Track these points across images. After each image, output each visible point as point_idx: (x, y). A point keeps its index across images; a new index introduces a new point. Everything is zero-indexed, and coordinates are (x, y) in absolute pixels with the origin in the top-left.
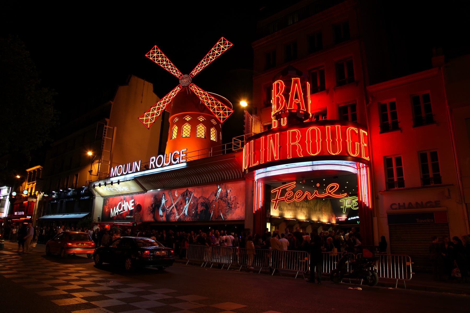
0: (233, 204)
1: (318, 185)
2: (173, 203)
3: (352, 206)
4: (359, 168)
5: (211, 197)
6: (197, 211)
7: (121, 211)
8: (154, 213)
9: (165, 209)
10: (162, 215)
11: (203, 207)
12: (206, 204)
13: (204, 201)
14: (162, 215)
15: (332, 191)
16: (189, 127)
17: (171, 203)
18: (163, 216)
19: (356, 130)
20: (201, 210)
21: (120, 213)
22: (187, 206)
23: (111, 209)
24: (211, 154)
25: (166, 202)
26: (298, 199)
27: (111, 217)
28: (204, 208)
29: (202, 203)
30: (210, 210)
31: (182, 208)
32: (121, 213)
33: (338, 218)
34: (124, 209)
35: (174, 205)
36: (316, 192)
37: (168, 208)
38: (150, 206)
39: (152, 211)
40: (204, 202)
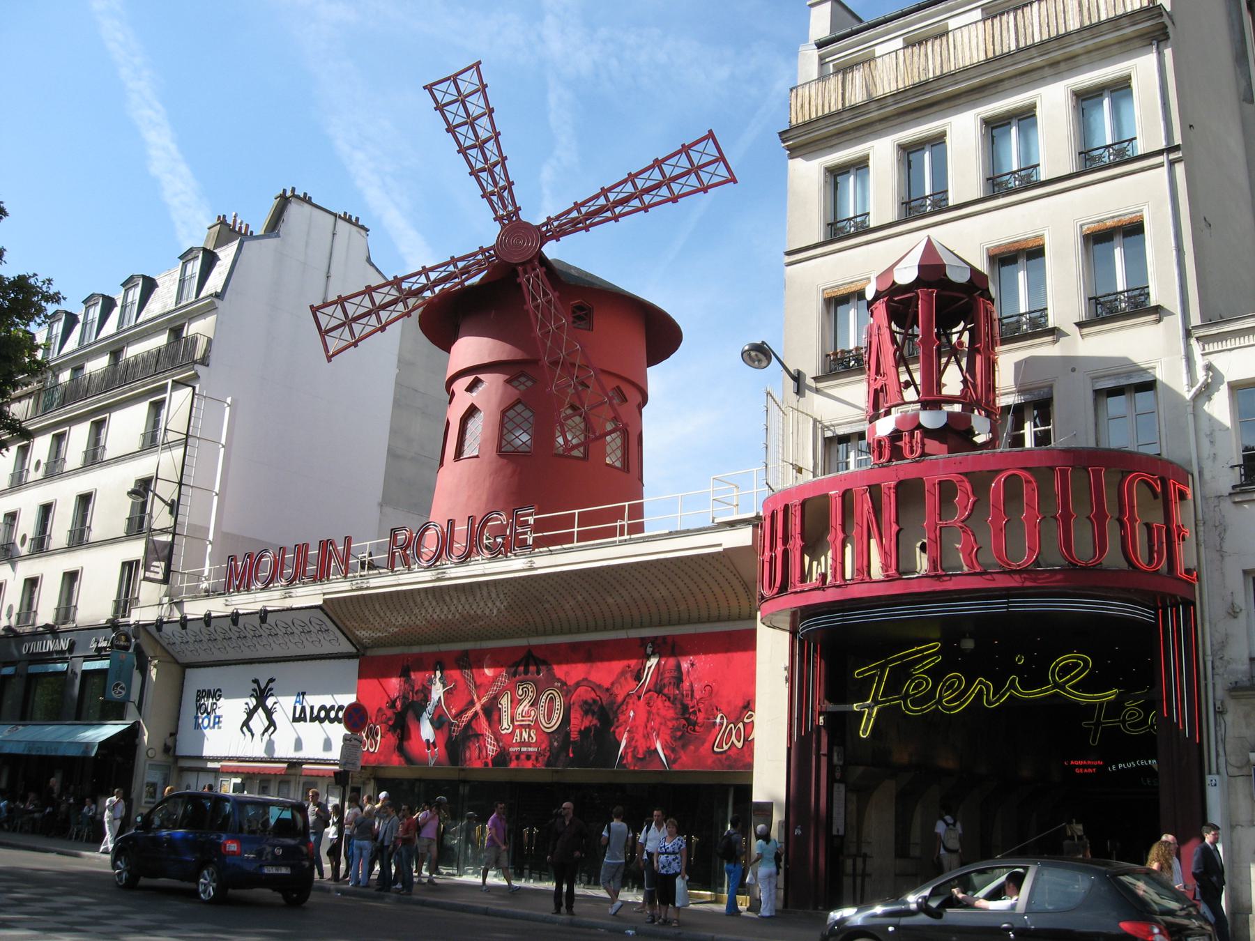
1: (1020, 660)
2: (475, 697)
3: (1124, 722)
4: (1160, 605)
5: (620, 683)
6: (567, 732)
9: (444, 718)
10: (431, 741)
11: (590, 717)
12: (602, 707)
13: (593, 695)
14: (431, 741)
15: (1070, 681)
16: (527, 414)
17: (469, 698)
18: (434, 743)
19: (1155, 481)
20: (583, 729)
24: (622, 527)
25: (447, 693)
26: (946, 702)
29: (586, 702)
30: (617, 730)
33: (1072, 762)
35: (478, 707)
36: (1014, 680)
37: (455, 717)
38: (384, 708)
40: (594, 700)
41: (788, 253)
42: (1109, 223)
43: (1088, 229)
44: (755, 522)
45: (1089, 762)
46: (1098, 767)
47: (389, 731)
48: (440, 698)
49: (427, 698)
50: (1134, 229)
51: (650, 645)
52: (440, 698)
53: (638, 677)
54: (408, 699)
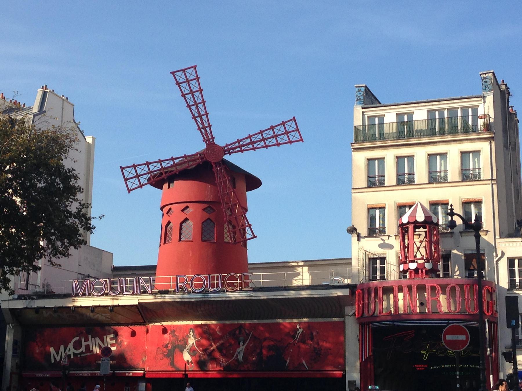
0: (322, 350)
7: (82, 353)
8: (173, 359)
10: (190, 361)
13: (272, 343)
14: (190, 361)
20: (268, 356)
21: (79, 356)
22: (242, 348)
23: (52, 350)
27: (53, 361)
28: (274, 353)
31: (231, 352)
32: (82, 355)
34: (91, 349)
39: (166, 354)
41: (353, 189)
42: (471, 200)
43: (464, 200)
44: (352, 288)
45: (422, 366)
46: (425, 367)
47: (165, 357)
48: (193, 343)
49: (186, 342)
50: (478, 203)
51: (298, 325)
52: (193, 343)
53: (293, 337)
54: (175, 344)
